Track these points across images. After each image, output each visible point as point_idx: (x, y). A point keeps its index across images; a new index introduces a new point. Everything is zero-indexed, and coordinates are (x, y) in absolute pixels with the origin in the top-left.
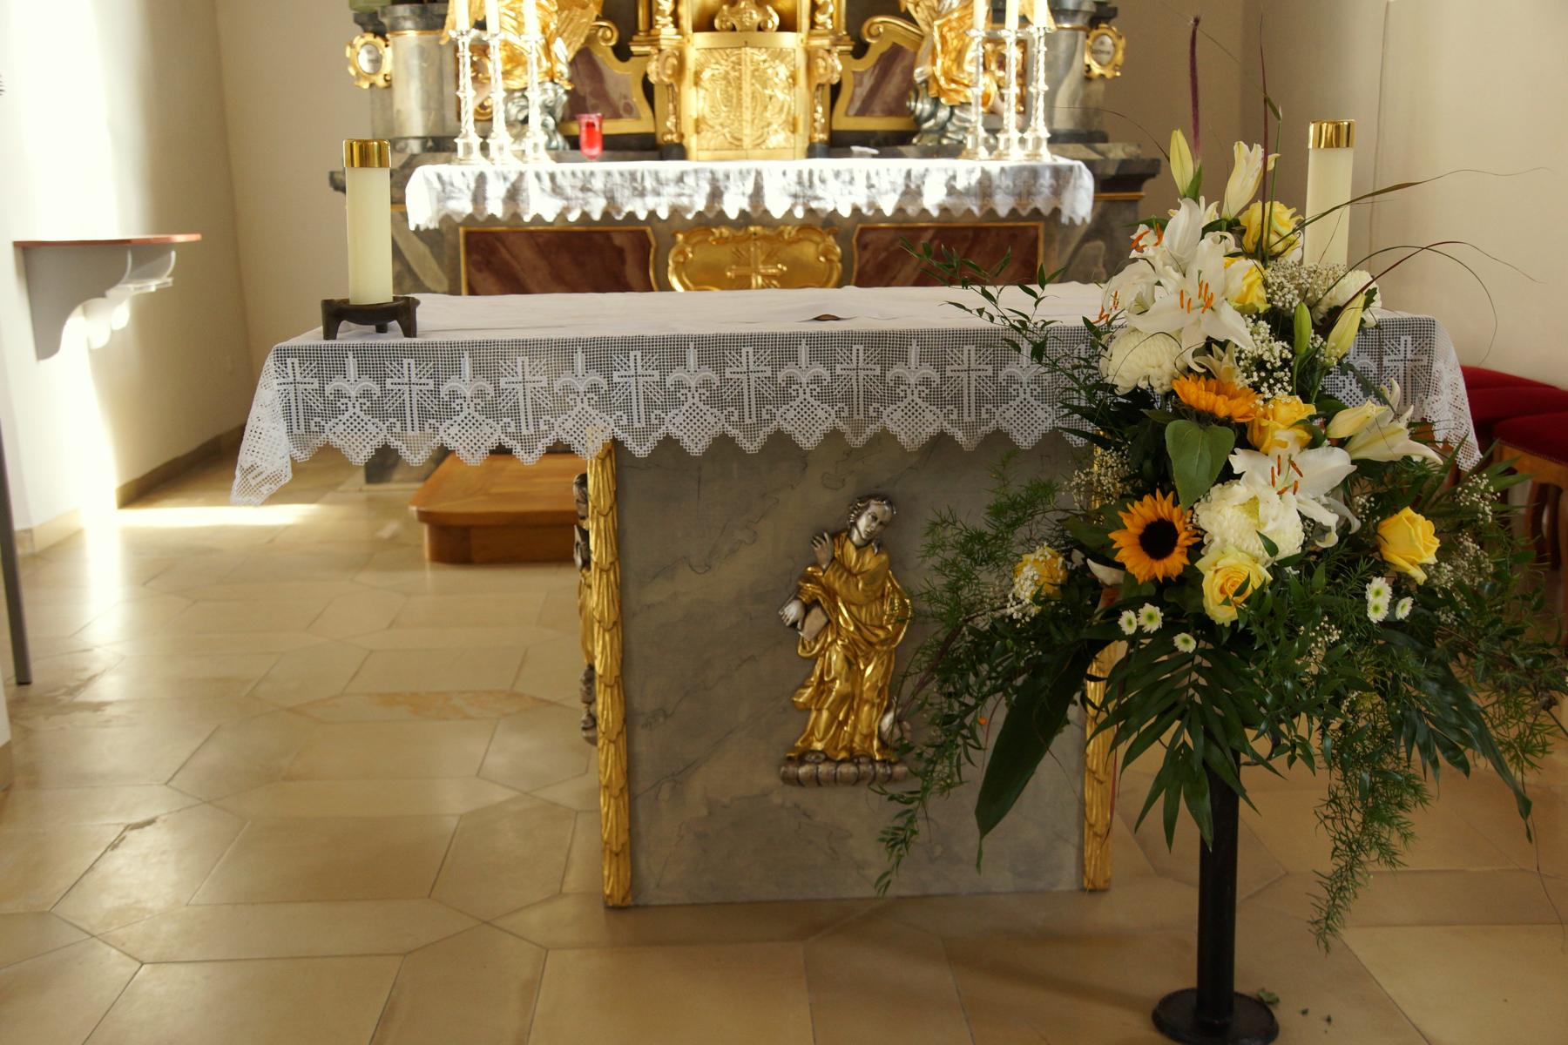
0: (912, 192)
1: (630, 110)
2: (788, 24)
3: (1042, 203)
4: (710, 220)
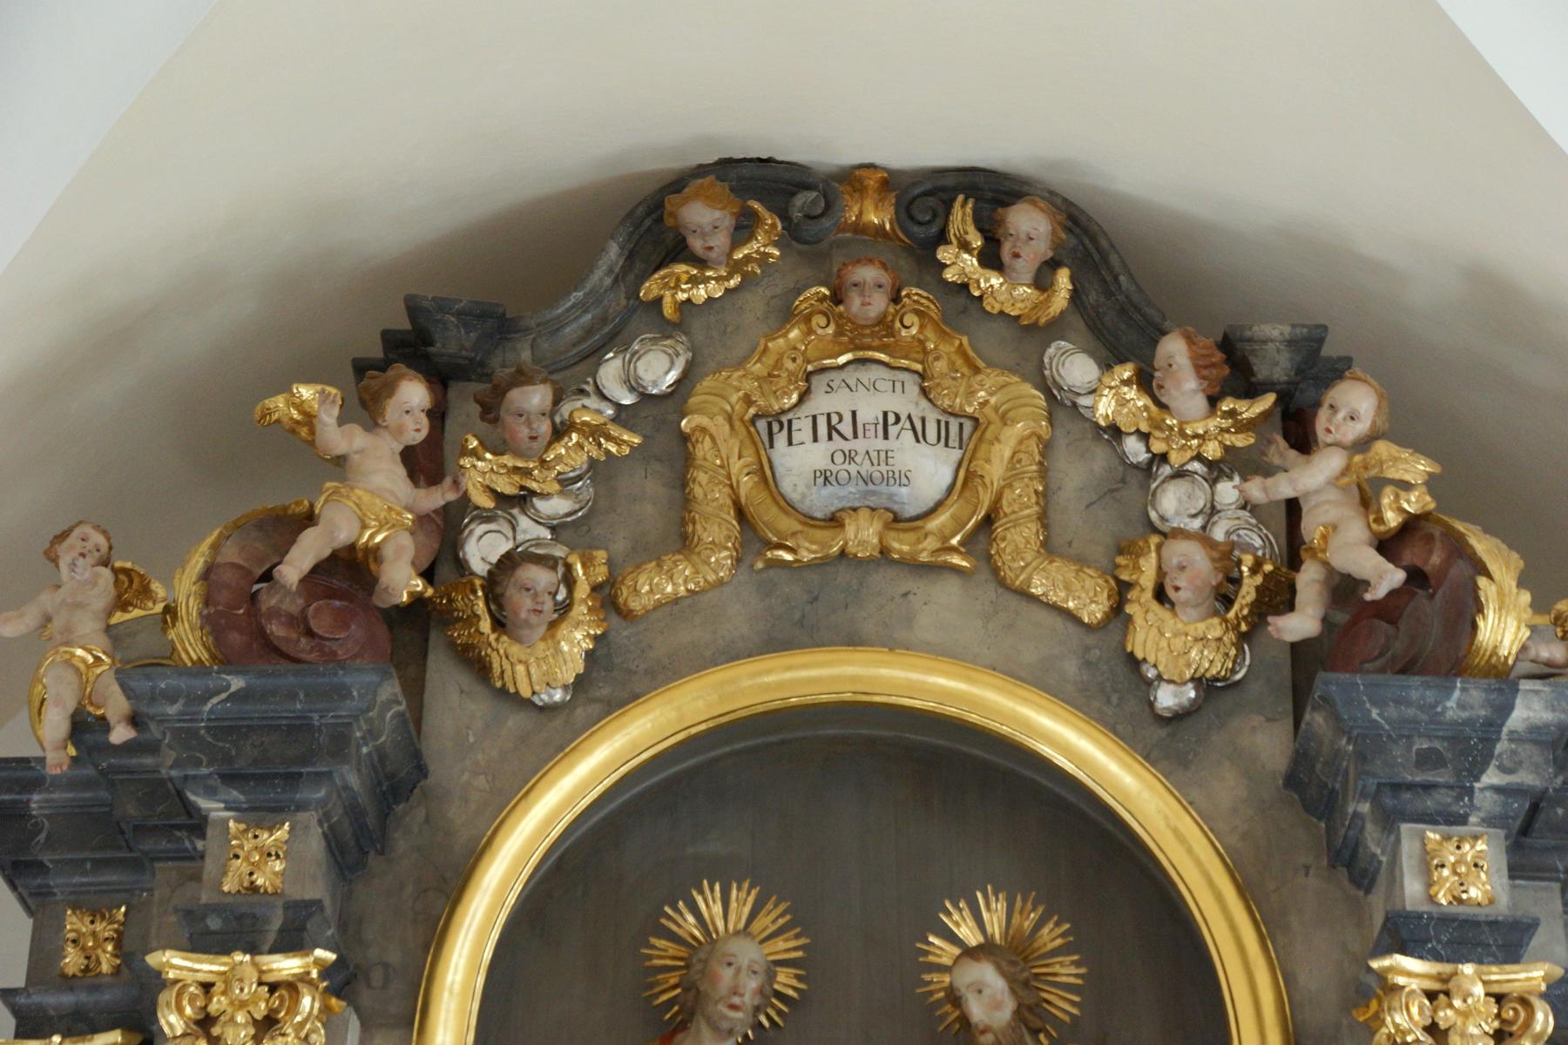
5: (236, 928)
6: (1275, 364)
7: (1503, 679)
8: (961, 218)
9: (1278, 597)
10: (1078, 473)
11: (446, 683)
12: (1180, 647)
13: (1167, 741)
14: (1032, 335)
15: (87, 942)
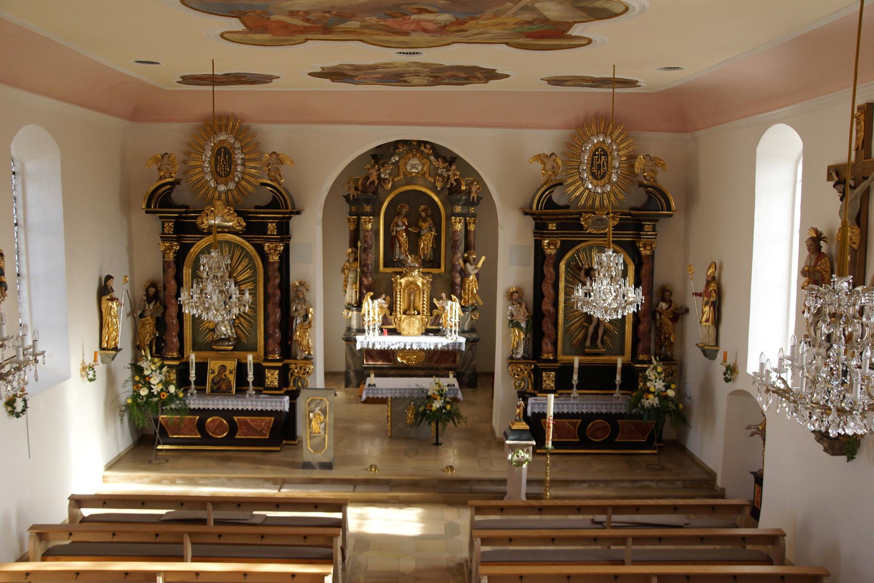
0: (436, 346)
1: (392, 324)
2: (419, 314)
3: (457, 348)
4: (405, 349)
10: (432, 168)
11: (380, 190)
12: (439, 185)
14: (429, 155)
15: (354, 209)
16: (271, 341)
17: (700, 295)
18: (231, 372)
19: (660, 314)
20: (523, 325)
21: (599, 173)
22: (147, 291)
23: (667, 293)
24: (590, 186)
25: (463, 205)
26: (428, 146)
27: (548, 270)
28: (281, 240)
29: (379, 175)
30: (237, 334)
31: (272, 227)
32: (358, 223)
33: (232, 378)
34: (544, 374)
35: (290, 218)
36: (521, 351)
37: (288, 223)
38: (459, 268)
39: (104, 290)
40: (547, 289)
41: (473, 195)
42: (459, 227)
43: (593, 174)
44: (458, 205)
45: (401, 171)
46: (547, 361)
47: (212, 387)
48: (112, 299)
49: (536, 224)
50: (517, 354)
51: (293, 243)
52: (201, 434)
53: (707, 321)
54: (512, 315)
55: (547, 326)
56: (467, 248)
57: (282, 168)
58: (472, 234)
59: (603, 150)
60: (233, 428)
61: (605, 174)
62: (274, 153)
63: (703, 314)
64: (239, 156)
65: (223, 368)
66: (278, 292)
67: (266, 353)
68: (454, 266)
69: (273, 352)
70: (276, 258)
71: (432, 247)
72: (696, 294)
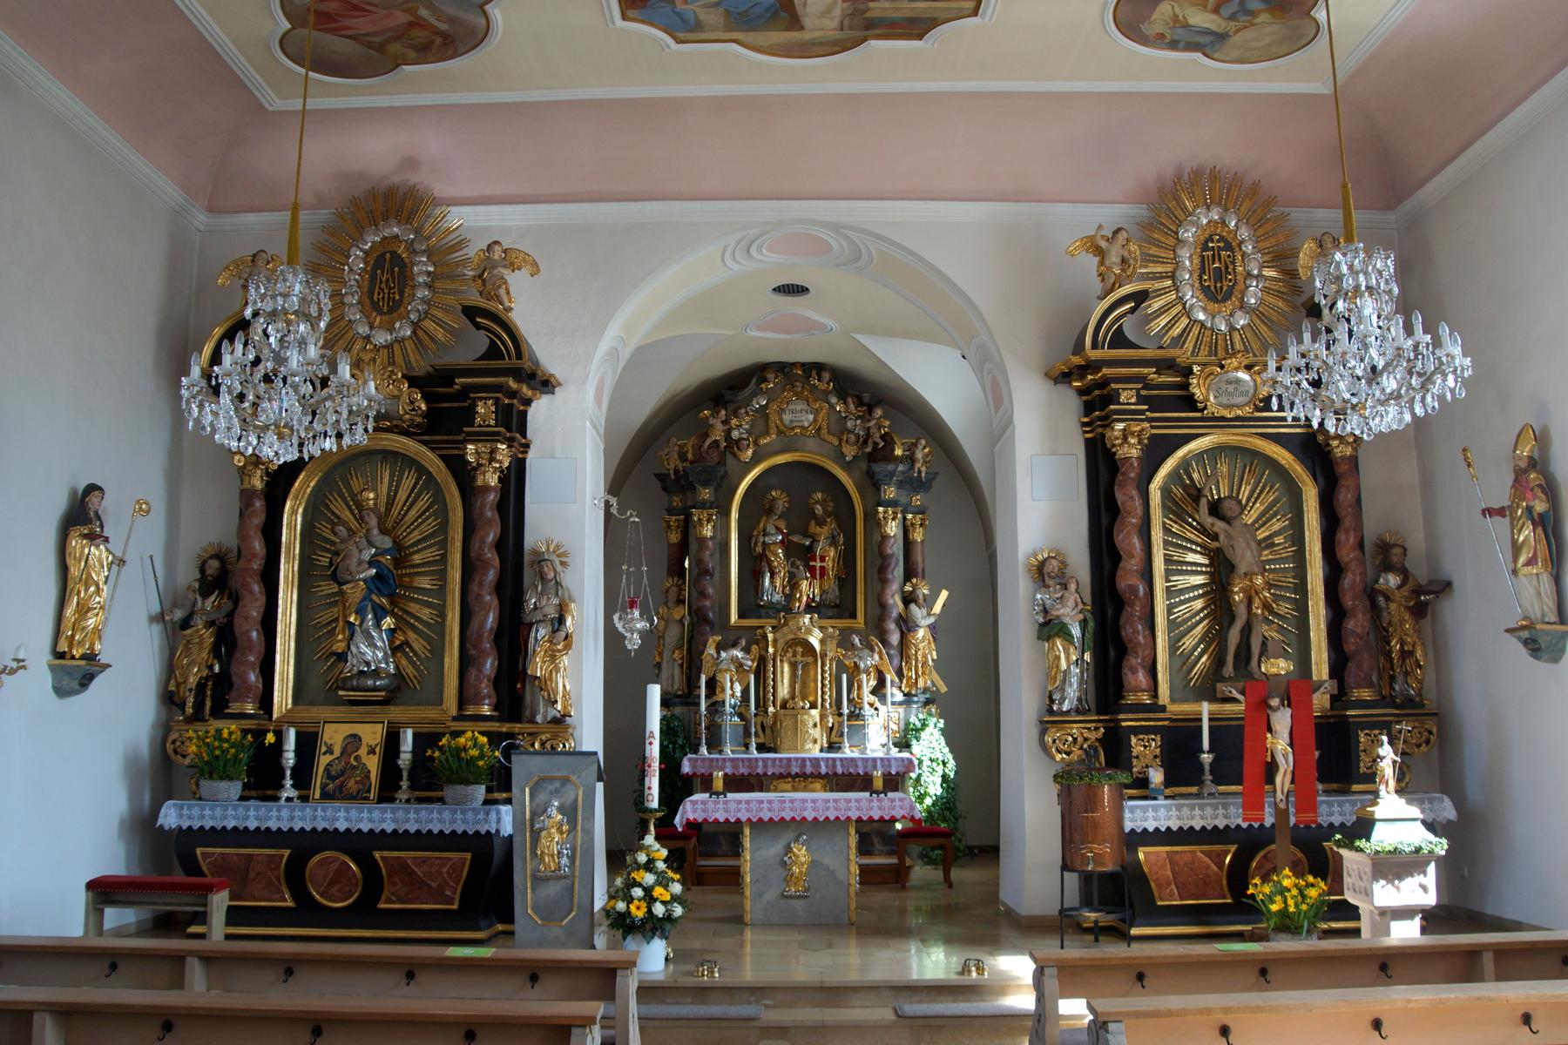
2: (813, 706)
5: (703, 505)
6: (866, 399)
7: (897, 458)
8: (814, 373)
9: (865, 442)
10: (833, 418)
12: (850, 452)
13: (847, 467)
14: (826, 392)
15: (677, 501)
16: (473, 673)
17: (1501, 512)
18: (372, 751)
19: (1388, 599)
20: (1076, 631)
21: (1219, 284)
22: (202, 570)
23: (1397, 550)
24: (1201, 316)
25: (900, 485)
26: (826, 376)
27: (1126, 496)
28: (510, 442)
29: (728, 432)
30: (397, 668)
31: (484, 410)
32: (687, 527)
33: (373, 764)
34: (1134, 740)
35: (528, 402)
36: (1072, 692)
37: (525, 413)
38: (895, 614)
39: (81, 515)
40: (1127, 540)
41: (918, 465)
42: (893, 528)
43: (1205, 290)
44: (889, 484)
45: (772, 425)
46: (1139, 708)
47: (324, 786)
48: (92, 537)
49: (1088, 408)
50: (1062, 702)
51: (532, 458)
52: (294, 898)
53: (1531, 562)
54: (1045, 611)
55: (1133, 630)
56: (909, 574)
57: (517, 281)
58: (919, 549)
59: (1222, 239)
60: (373, 882)
61: (1231, 289)
62: (496, 243)
63: (1516, 549)
64: (422, 268)
65: (355, 739)
66: (492, 556)
67: (462, 702)
68: (883, 606)
69: (478, 701)
70: (493, 480)
71: (838, 578)
72: (1488, 512)
